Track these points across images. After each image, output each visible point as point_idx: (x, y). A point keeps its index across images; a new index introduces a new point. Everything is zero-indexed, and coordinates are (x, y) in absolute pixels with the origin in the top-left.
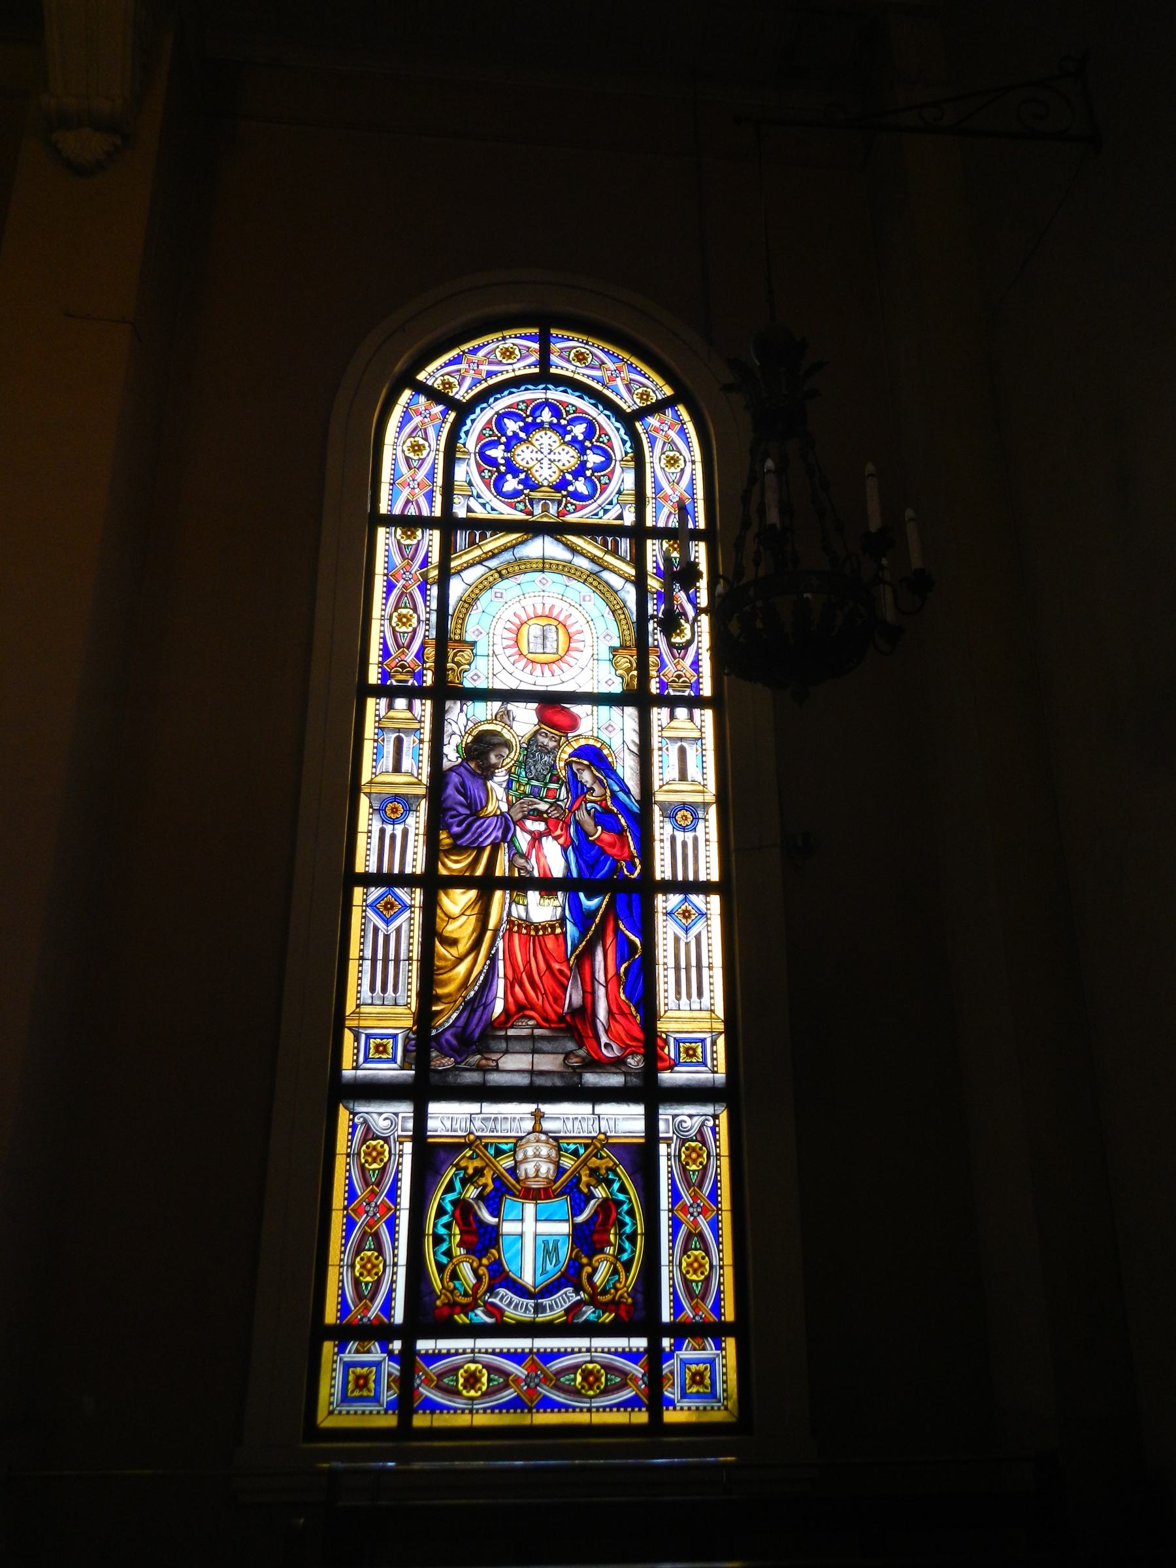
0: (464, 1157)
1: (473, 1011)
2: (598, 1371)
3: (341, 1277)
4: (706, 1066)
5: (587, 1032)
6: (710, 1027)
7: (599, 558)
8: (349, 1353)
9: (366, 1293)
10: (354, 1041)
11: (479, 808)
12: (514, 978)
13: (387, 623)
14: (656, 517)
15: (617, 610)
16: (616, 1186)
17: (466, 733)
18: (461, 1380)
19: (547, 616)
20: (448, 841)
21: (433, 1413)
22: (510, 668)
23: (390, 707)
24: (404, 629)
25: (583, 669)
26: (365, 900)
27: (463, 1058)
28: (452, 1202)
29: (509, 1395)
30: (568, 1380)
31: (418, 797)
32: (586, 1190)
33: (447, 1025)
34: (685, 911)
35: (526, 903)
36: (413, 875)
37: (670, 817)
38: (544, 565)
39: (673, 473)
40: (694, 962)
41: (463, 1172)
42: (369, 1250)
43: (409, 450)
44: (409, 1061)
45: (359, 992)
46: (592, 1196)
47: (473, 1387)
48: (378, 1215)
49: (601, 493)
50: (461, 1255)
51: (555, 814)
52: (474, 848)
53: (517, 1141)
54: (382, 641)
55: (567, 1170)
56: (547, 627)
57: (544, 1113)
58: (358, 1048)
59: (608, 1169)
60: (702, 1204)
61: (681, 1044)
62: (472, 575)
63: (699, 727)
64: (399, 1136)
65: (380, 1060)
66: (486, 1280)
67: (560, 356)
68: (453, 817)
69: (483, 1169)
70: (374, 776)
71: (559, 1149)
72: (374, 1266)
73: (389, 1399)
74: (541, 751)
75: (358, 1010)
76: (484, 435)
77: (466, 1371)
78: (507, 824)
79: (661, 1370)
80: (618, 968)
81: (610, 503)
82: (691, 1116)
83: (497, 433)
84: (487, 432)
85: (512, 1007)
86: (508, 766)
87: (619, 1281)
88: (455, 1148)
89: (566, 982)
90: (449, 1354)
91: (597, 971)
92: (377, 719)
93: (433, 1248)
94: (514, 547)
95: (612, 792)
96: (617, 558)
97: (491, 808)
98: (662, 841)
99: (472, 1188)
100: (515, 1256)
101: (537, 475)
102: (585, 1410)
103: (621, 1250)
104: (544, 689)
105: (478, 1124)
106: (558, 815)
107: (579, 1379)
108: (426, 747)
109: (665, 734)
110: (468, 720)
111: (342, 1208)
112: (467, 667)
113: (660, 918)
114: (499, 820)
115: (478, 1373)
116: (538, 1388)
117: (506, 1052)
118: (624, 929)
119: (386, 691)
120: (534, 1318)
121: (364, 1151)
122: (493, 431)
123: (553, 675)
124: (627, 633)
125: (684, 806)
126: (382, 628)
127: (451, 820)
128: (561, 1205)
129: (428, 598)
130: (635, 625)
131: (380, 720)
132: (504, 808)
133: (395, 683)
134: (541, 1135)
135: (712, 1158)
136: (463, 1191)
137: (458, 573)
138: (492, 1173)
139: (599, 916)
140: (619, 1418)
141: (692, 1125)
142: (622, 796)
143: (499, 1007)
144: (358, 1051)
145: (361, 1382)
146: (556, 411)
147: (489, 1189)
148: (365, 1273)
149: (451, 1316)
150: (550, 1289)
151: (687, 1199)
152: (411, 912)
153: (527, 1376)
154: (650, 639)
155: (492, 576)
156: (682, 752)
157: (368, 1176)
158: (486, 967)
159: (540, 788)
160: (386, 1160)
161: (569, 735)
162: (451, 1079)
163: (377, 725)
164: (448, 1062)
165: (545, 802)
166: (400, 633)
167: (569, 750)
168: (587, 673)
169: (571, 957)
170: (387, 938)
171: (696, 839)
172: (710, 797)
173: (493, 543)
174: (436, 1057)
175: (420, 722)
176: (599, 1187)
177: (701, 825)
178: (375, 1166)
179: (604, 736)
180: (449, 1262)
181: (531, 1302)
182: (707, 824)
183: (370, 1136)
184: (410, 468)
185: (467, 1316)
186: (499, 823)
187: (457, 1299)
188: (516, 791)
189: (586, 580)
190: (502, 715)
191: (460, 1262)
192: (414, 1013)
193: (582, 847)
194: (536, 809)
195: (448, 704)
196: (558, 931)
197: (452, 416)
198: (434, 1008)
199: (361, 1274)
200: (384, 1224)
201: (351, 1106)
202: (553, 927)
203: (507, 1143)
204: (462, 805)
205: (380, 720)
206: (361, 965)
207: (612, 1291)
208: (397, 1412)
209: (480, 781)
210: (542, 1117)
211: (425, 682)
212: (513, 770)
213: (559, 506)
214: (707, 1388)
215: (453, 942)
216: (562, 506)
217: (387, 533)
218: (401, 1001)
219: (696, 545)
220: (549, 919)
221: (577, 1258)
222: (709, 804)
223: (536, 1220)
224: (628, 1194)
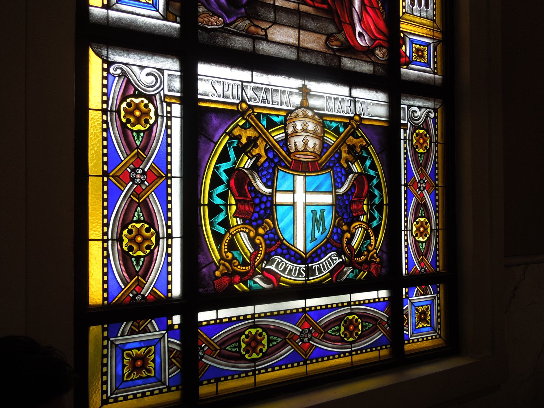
0: (237, 125)
2: (357, 320)
3: (105, 253)
4: (430, 67)
6: (432, 34)
8: (122, 335)
16: (368, 163)
21: (218, 381)
27: (232, 20)
29: (287, 351)
30: (334, 331)
42: (138, 221)
46: (349, 171)
47: (254, 350)
50: (238, 225)
53: (287, 114)
55: (331, 146)
57: (310, 90)
59: (363, 148)
61: (414, 45)
64: (165, 96)
66: (262, 249)
69: (256, 139)
71: (324, 126)
72: (145, 239)
77: (247, 336)
82: (420, 108)
93: (210, 219)
99: (246, 158)
100: (288, 225)
103: (372, 218)
105: (250, 93)
115: (259, 338)
116: (310, 342)
117: (274, 23)
120: (306, 280)
121: (125, 109)
134: (308, 111)
135: (433, 144)
138: (265, 143)
140: (373, 355)
147: (262, 160)
148: (135, 247)
149: (231, 284)
150: (317, 255)
153: (301, 333)
160: (151, 122)
162: (220, 40)
164: (216, 22)
174: (204, 13)
178: (138, 127)
180: (226, 232)
185: (246, 284)
191: (237, 233)
199: (131, 249)
201: (104, 52)
203: (278, 116)
207: (366, 253)
214: (428, 324)
223: (306, 192)
224: (377, 171)
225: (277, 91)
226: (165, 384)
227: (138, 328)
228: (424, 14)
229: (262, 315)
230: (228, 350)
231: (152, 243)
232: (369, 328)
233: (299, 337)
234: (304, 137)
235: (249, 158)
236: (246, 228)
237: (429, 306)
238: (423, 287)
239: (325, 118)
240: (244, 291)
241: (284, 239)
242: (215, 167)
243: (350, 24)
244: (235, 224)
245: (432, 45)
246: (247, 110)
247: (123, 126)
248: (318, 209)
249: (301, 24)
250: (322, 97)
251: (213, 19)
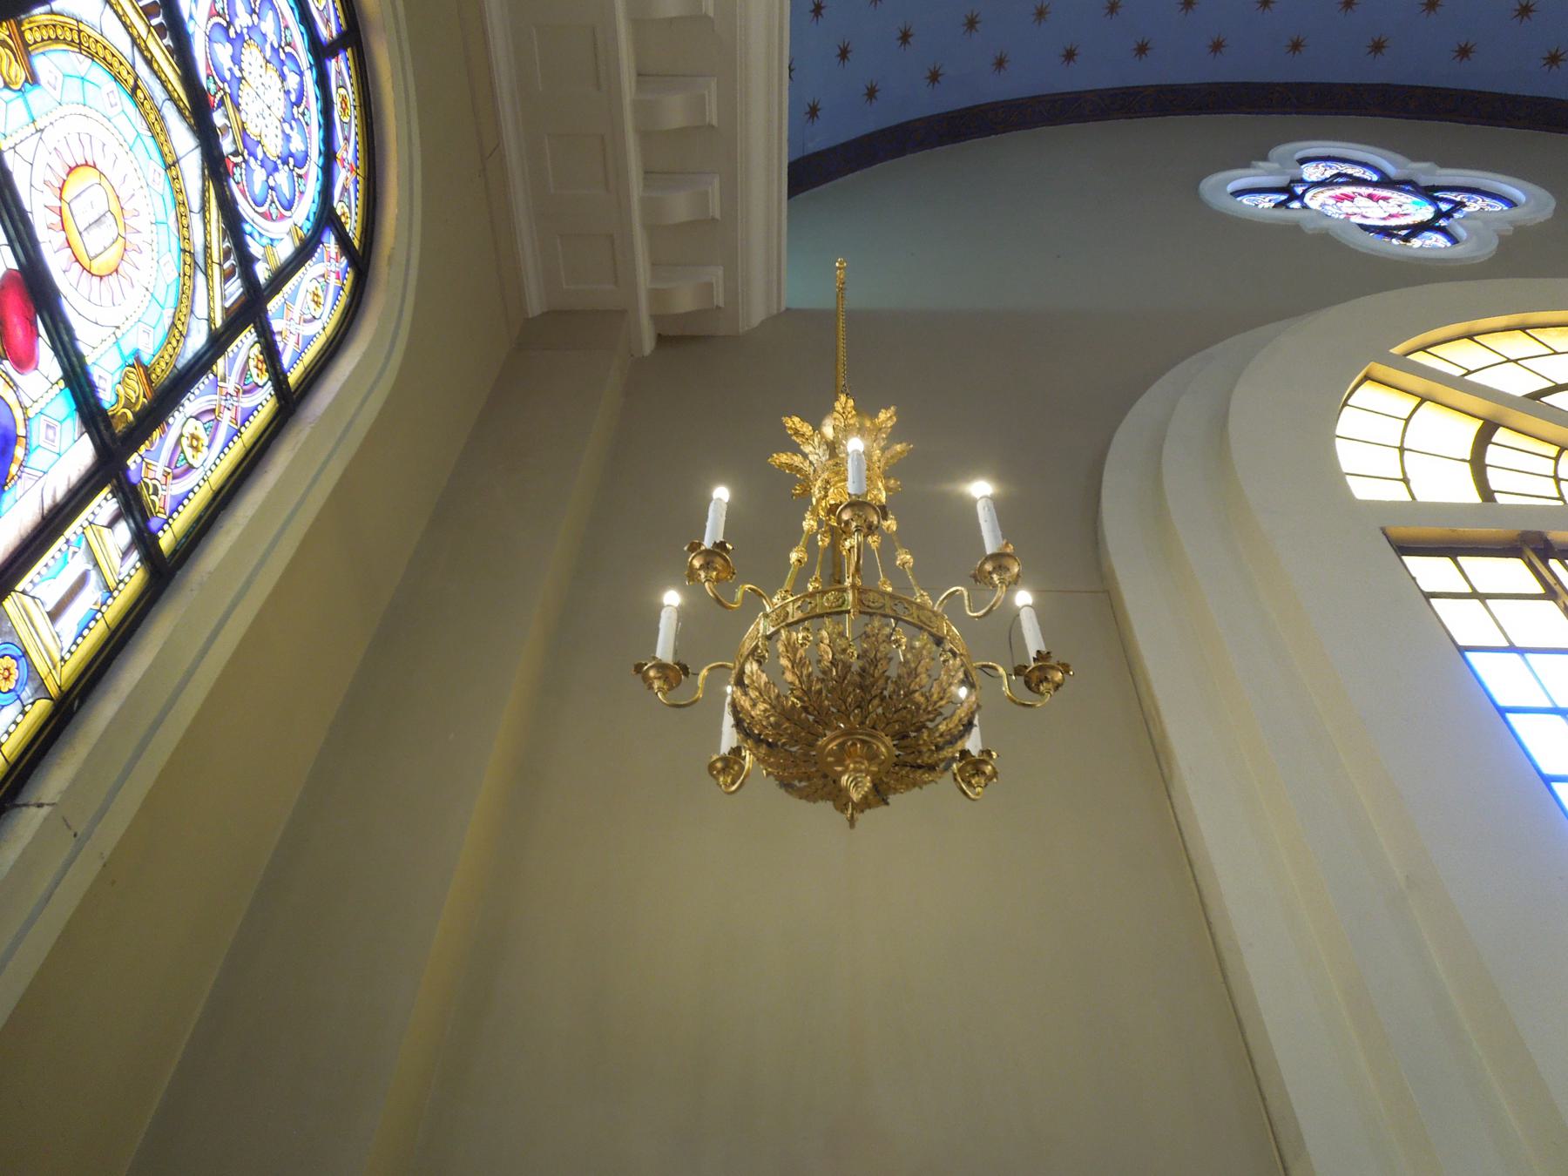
7: (211, 255)
15: (177, 331)
94: (171, 98)
124: (163, 365)
156: (82, 581)
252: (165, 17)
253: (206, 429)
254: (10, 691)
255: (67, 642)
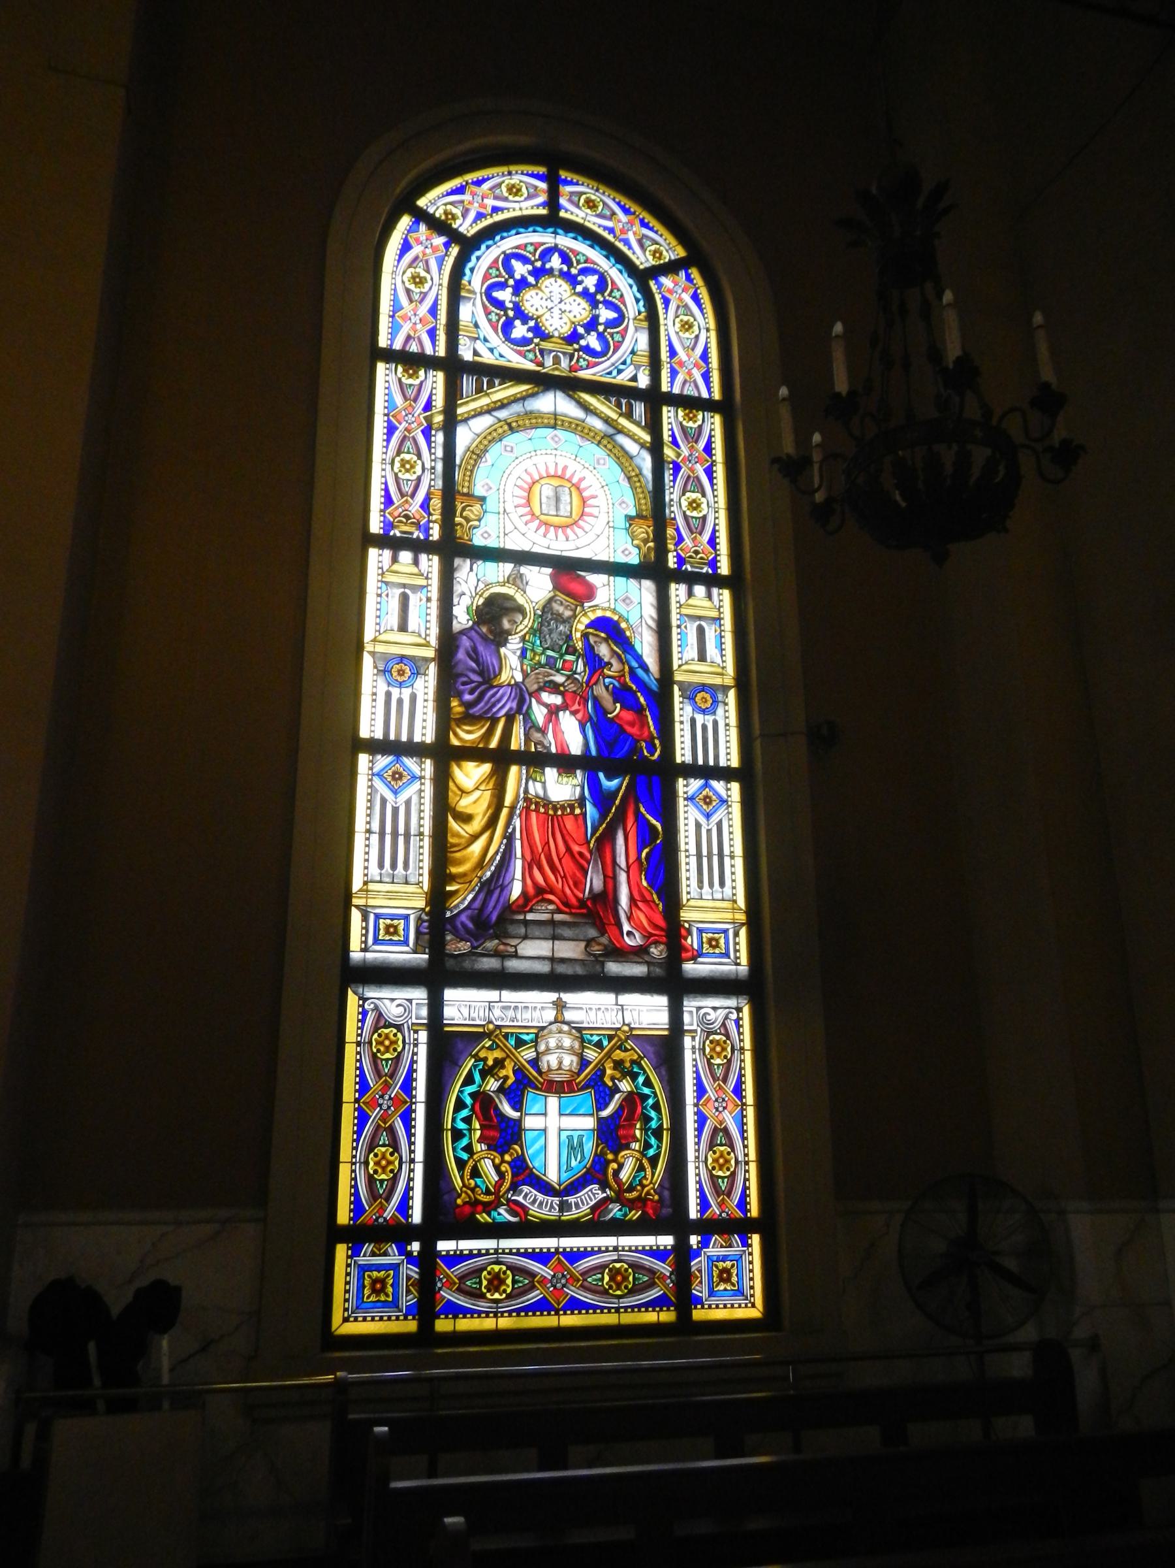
0: (483, 1047)
1: (490, 893)
3: (353, 1175)
4: (729, 958)
5: (609, 920)
6: (731, 917)
7: (613, 420)
9: (381, 1192)
10: (362, 921)
11: (492, 676)
12: (532, 860)
13: (388, 467)
14: (672, 383)
15: (633, 477)
16: (641, 1079)
17: (476, 594)
18: (485, 1283)
19: (559, 477)
20: (460, 709)
21: (455, 1317)
22: (523, 529)
23: (395, 560)
24: (407, 476)
25: (599, 536)
26: (371, 769)
27: (481, 942)
28: (471, 1095)
29: (534, 1296)
30: (596, 1280)
31: (426, 660)
32: (610, 1084)
33: (462, 907)
34: (706, 797)
35: (543, 780)
36: (423, 744)
37: (689, 699)
38: (555, 421)
39: (688, 339)
40: (715, 850)
41: (482, 1063)
43: (409, 281)
44: (423, 944)
45: (366, 868)
46: (617, 1090)
47: (497, 1290)
48: (392, 1108)
49: (614, 352)
50: (482, 1151)
51: (572, 687)
52: (488, 718)
53: (539, 1031)
54: (383, 487)
55: (591, 1063)
56: (561, 488)
58: (366, 928)
59: (633, 1062)
60: (726, 1099)
61: (704, 935)
62: (482, 424)
63: (718, 607)
64: (413, 1024)
65: (391, 943)
66: (509, 1177)
67: (570, 201)
68: (464, 684)
69: (504, 1060)
70: (378, 633)
71: (582, 1040)
72: (389, 1163)
73: (408, 1304)
74: (556, 621)
75: (365, 887)
76: (491, 274)
77: (489, 1273)
78: (522, 696)
79: (690, 1267)
80: (639, 852)
81: (624, 363)
82: (715, 1009)
83: (504, 274)
84: (494, 272)
85: (531, 890)
86: (522, 633)
87: (645, 1177)
88: (473, 1038)
89: (586, 865)
90: (471, 1255)
91: (618, 856)
92: (380, 571)
93: (452, 1144)
95: (632, 670)
96: (631, 422)
97: (504, 677)
98: (682, 723)
99: (492, 1080)
100: (538, 1152)
101: (547, 324)
102: (613, 1310)
103: (647, 1146)
104: (558, 553)
105: (497, 1012)
106: (575, 689)
107: (607, 1278)
108: (434, 605)
109: (684, 611)
110: (478, 580)
111: (353, 1100)
112: (476, 523)
113: (681, 802)
114: (514, 690)
115: (502, 1276)
117: (525, 937)
118: (644, 812)
119: (385, 541)
120: (560, 1216)
121: (376, 1040)
122: (500, 272)
123: (567, 540)
124: (643, 501)
125: (704, 687)
126: (383, 473)
127: (462, 687)
128: (586, 1099)
129: (433, 445)
130: (651, 494)
131: (383, 573)
132: (519, 677)
133: (398, 534)
136: (483, 1083)
137: (466, 420)
138: (513, 1064)
139: (619, 798)
140: (651, 1317)
141: (716, 1017)
142: (640, 672)
143: (516, 891)
144: (367, 931)
145: (378, 1286)
146: (565, 259)
147: (510, 1082)
148: (380, 1171)
149: (473, 1214)
150: (575, 1187)
151: (711, 1093)
152: (422, 784)
153: (553, 1276)
154: (667, 511)
155: (501, 427)
156: (701, 632)
157: (380, 1067)
158: (503, 847)
159: (555, 659)
160: (399, 1049)
161: (586, 604)
162: (467, 964)
163: (380, 578)
164: (464, 947)
165: (562, 674)
166: (403, 480)
167: (586, 621)
168: (603, 540)
169: (591, 839)
170: (395, 811)
171: (715, 723)
172: (729, 681)
173: (503, 392)
174: (451, 940)
175: (427, 578)
176: (624, 1081)
177: (720, 711)
178: (387, 1056)
179: (622, 608)
180: (469, 1158)
181: (556, 1200)
182: (727, 708)
183: (382, 1023)
184: (411, 301)
185: (489, 1215)
186: (513, 694)
187: (478, 1197)
188: (531, 660)
189: (599, 442)
190: (515, 579)
192: (426, 893)
193: (600, 724)
194: (551, 682)
195: (457, 561)
196: (578, 811)
197: (455, 250)
198: (448, 888)
199: (376, 1172)
200: (398, 1118)
201: (360, 990)
202: (572, 807)
203: (528, 1034)
204: (474, 671)
205: (383, 573)
206: (368, 839)
207: (639, 1188)
208: (417, 1317)
209: (493, 647)
210: (564, 1007)
211: (432, 535)
212: (527, 638)
213: (571, 360)
214: (734, 1286)
215: (466, 818)
216: (575, 360)
217: (387, 369)
218: (412, 879)
219: (712, 417)
220: (568, 799)
221: (603, 1154)
222: (728, 688)
223: (561, 1115)
224: (653, 1088)
225: (526, 1007)
226: (402, 1312)
227: (380, 1250)
228: (719, 896)
229: (507, 1251)
230: (467, 1285)
231: (395, 1167)
232: (644, 1282)
233: (551, 1281)
234: (557, 1054)
235: (496, 1080)
236: (492, 1155)
237: (735, 1262)
238: (726, 1236)
239: (584, 1032)
240: (487, 1223)
241: (534, 1167)
242: (459, 1091)
243: (615, 925)
244: (479, 1150)
245: (731, 933)
246: (494, 1031)
247: (374, 1056)
248: (576, 1134)
249: (556, 933)
250: (581, 1008)
251: (461, 944)
252: (485, 377)
253: (693, 492)
254: (712, 705)
255: (718, 660)
